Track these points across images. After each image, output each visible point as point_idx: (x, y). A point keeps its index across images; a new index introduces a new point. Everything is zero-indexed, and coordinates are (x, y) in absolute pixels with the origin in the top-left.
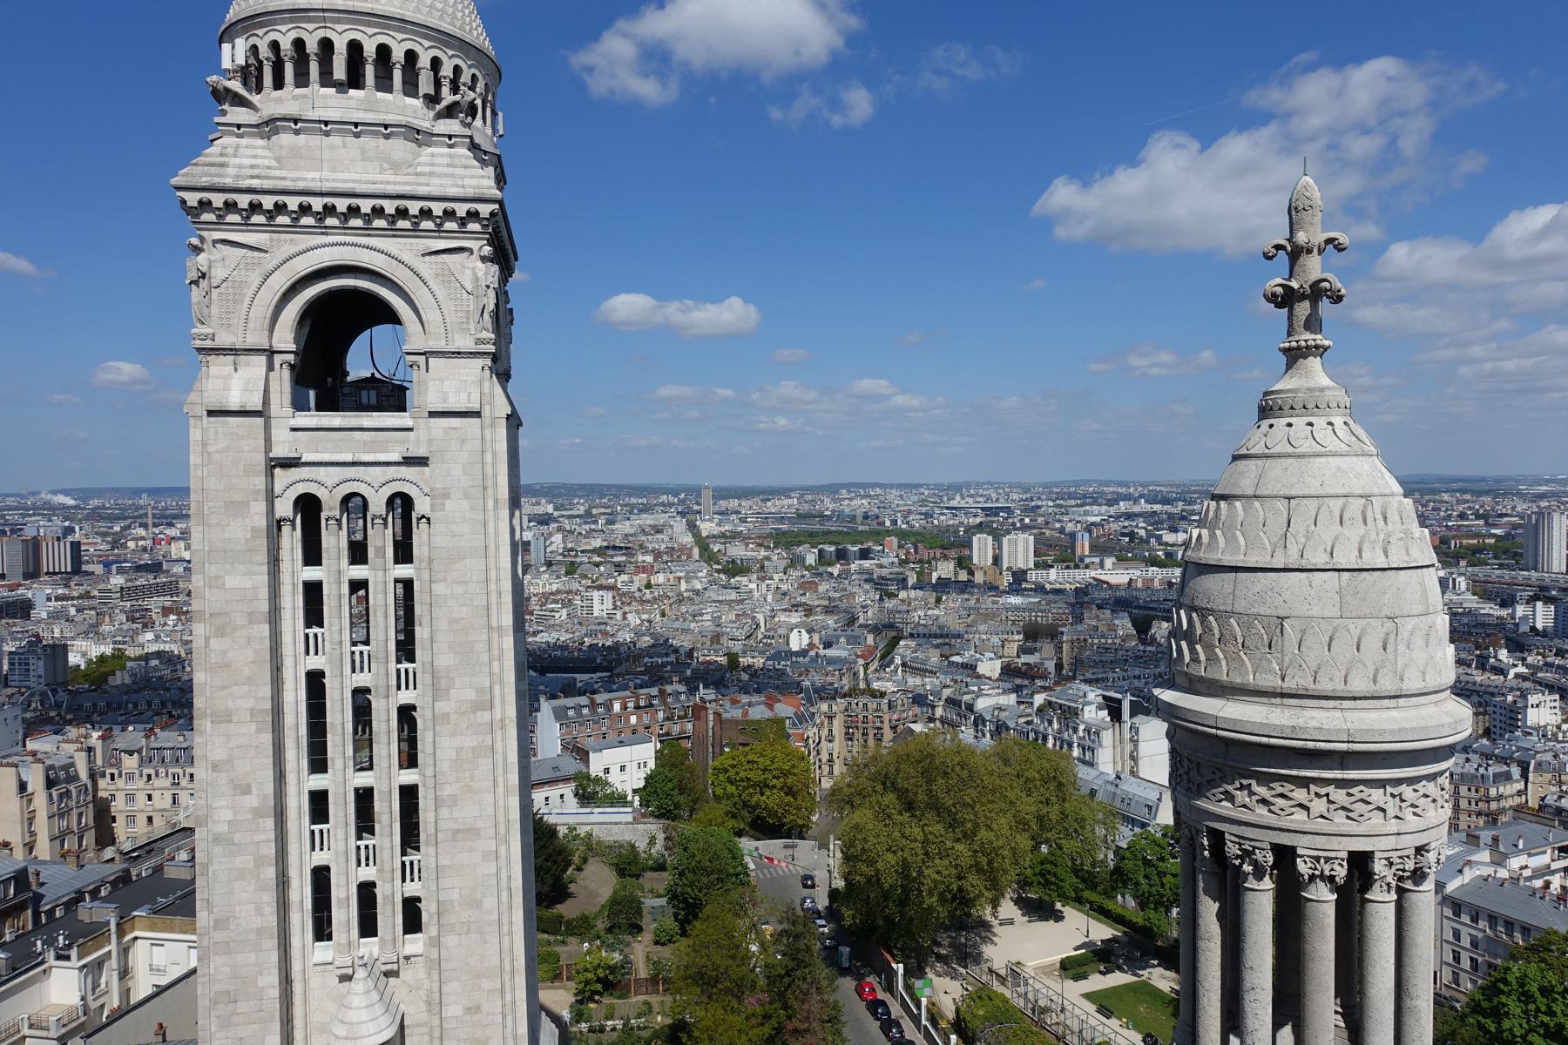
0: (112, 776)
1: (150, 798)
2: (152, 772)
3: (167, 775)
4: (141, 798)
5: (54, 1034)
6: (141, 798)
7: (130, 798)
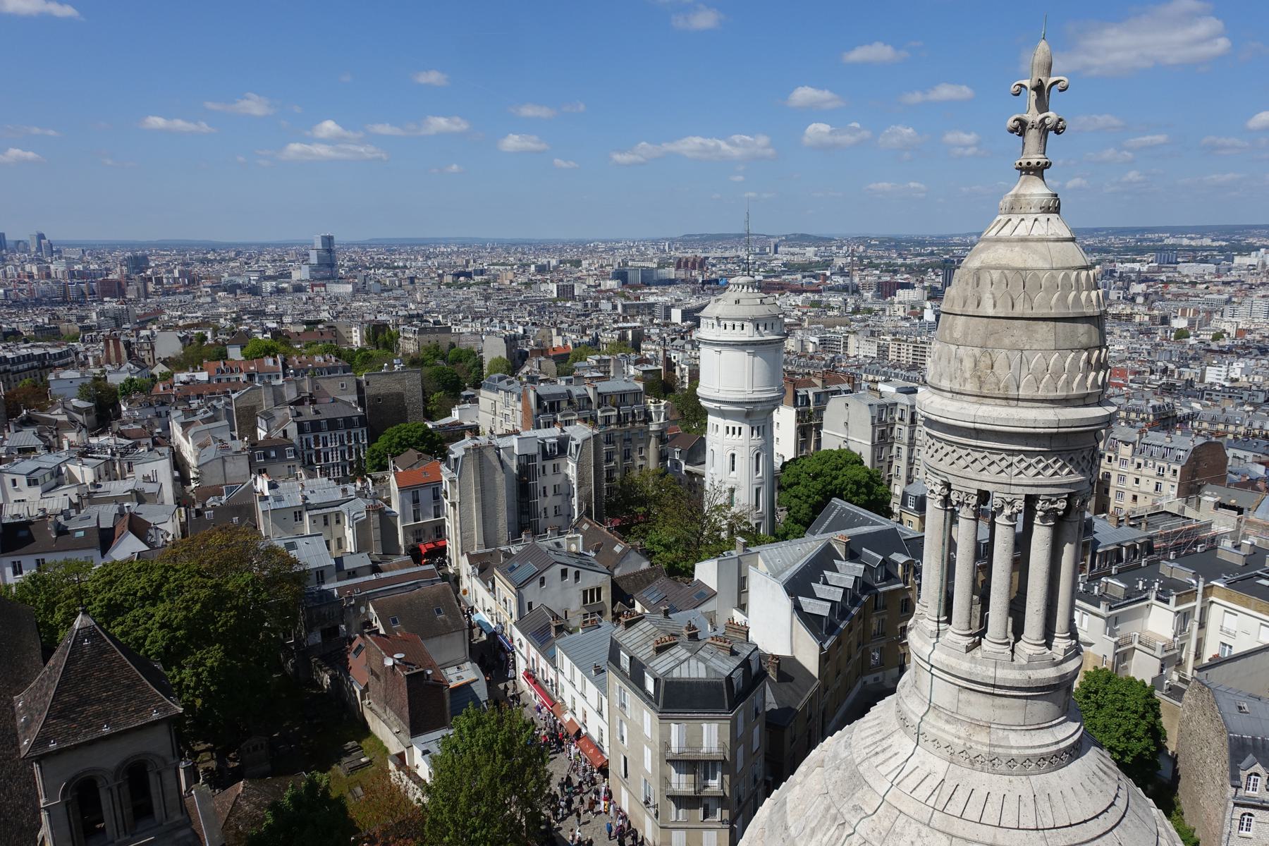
0: (1110, 458)
1: (1137, 481)
2: (1142, 462)
3: (1154, 466)
4: (1130, 480)
5: (1158, 653)
6: (1130, 480)
7: (1122, 478)
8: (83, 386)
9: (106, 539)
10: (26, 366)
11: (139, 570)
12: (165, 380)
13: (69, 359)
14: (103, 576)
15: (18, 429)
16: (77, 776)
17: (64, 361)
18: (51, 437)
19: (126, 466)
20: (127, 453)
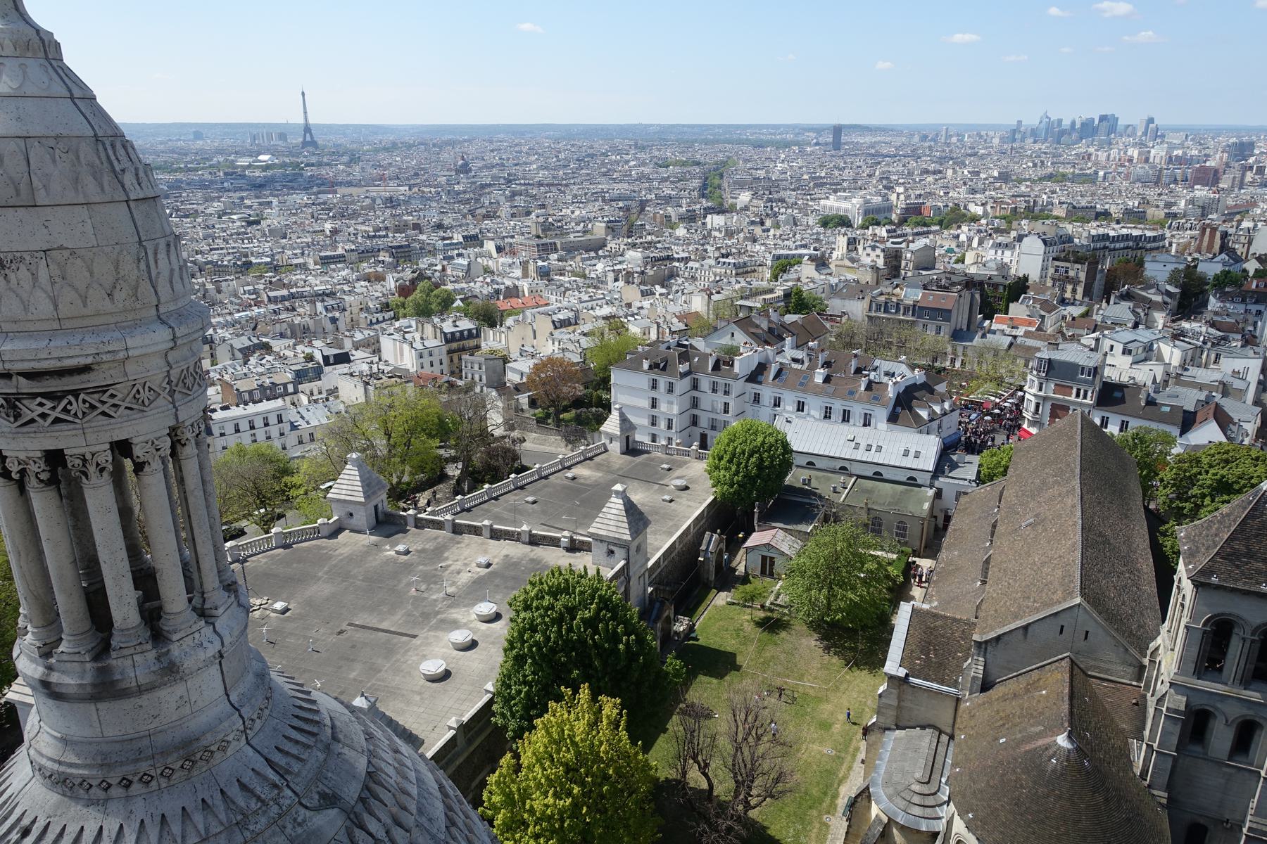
8: (1176, 271)
9: (1188, 421)
10: (1122, 245)
11: (1257, 459)
12: (1261, 277)
13: (1161, 244)
14: (1219, 453)
15: (1117, 301)
16: (1223, 614)
17: (1155, 245)
18: (1142, 314)
19: (1213, 356)
20: (1218, 344)
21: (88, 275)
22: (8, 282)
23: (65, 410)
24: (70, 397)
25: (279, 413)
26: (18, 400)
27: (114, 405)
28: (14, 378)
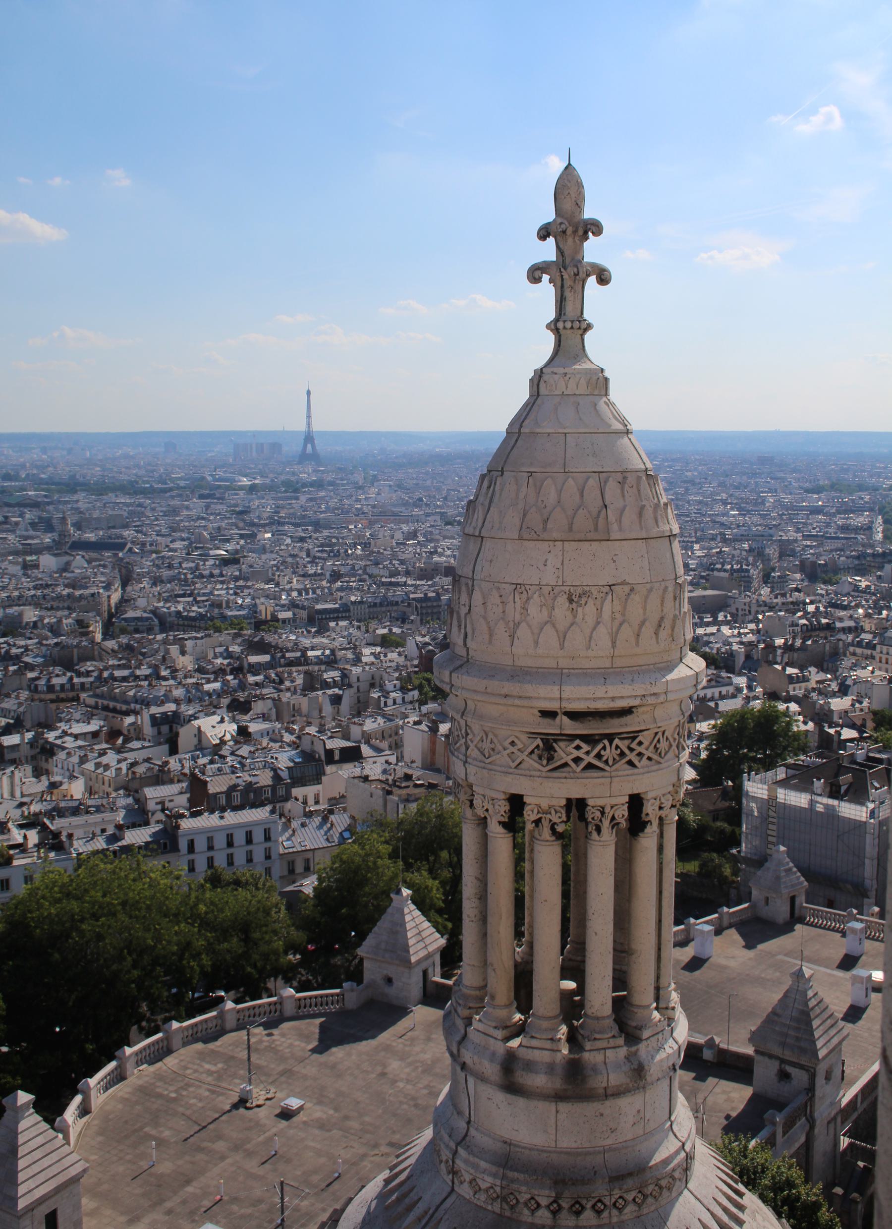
21: (641, 611)
22: (575, 617)
23: (599, 756)
24: (606, 742)
25: (267, 826)
26: (555, 741)
27: (640, 754)
28: (558, 718)
